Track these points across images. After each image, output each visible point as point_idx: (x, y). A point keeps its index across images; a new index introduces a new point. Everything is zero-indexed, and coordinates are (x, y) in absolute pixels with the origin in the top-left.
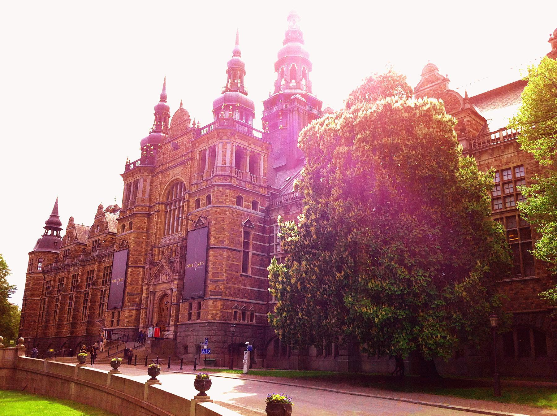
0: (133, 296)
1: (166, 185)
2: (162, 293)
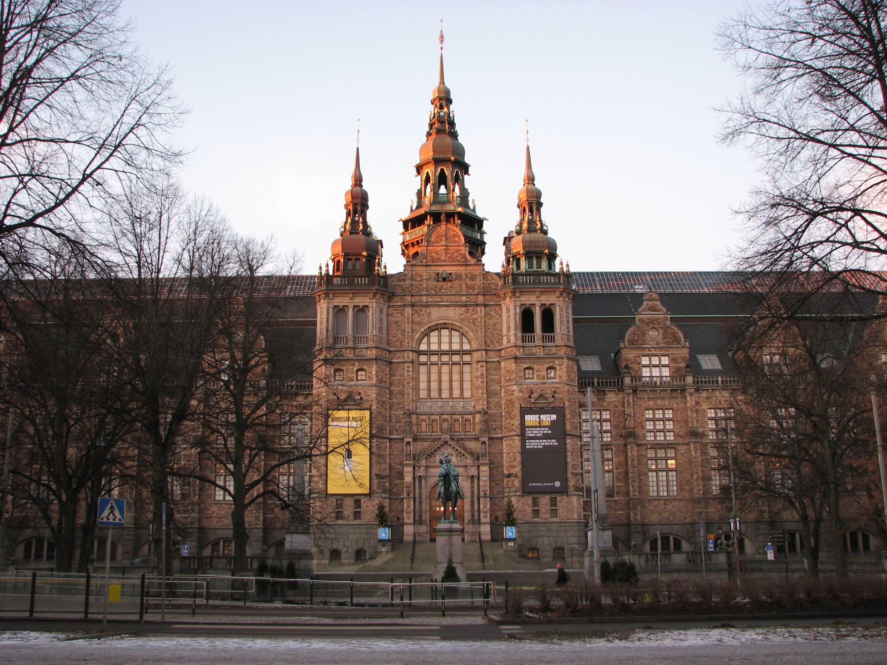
0: (382, 478)
1: (426, 327)
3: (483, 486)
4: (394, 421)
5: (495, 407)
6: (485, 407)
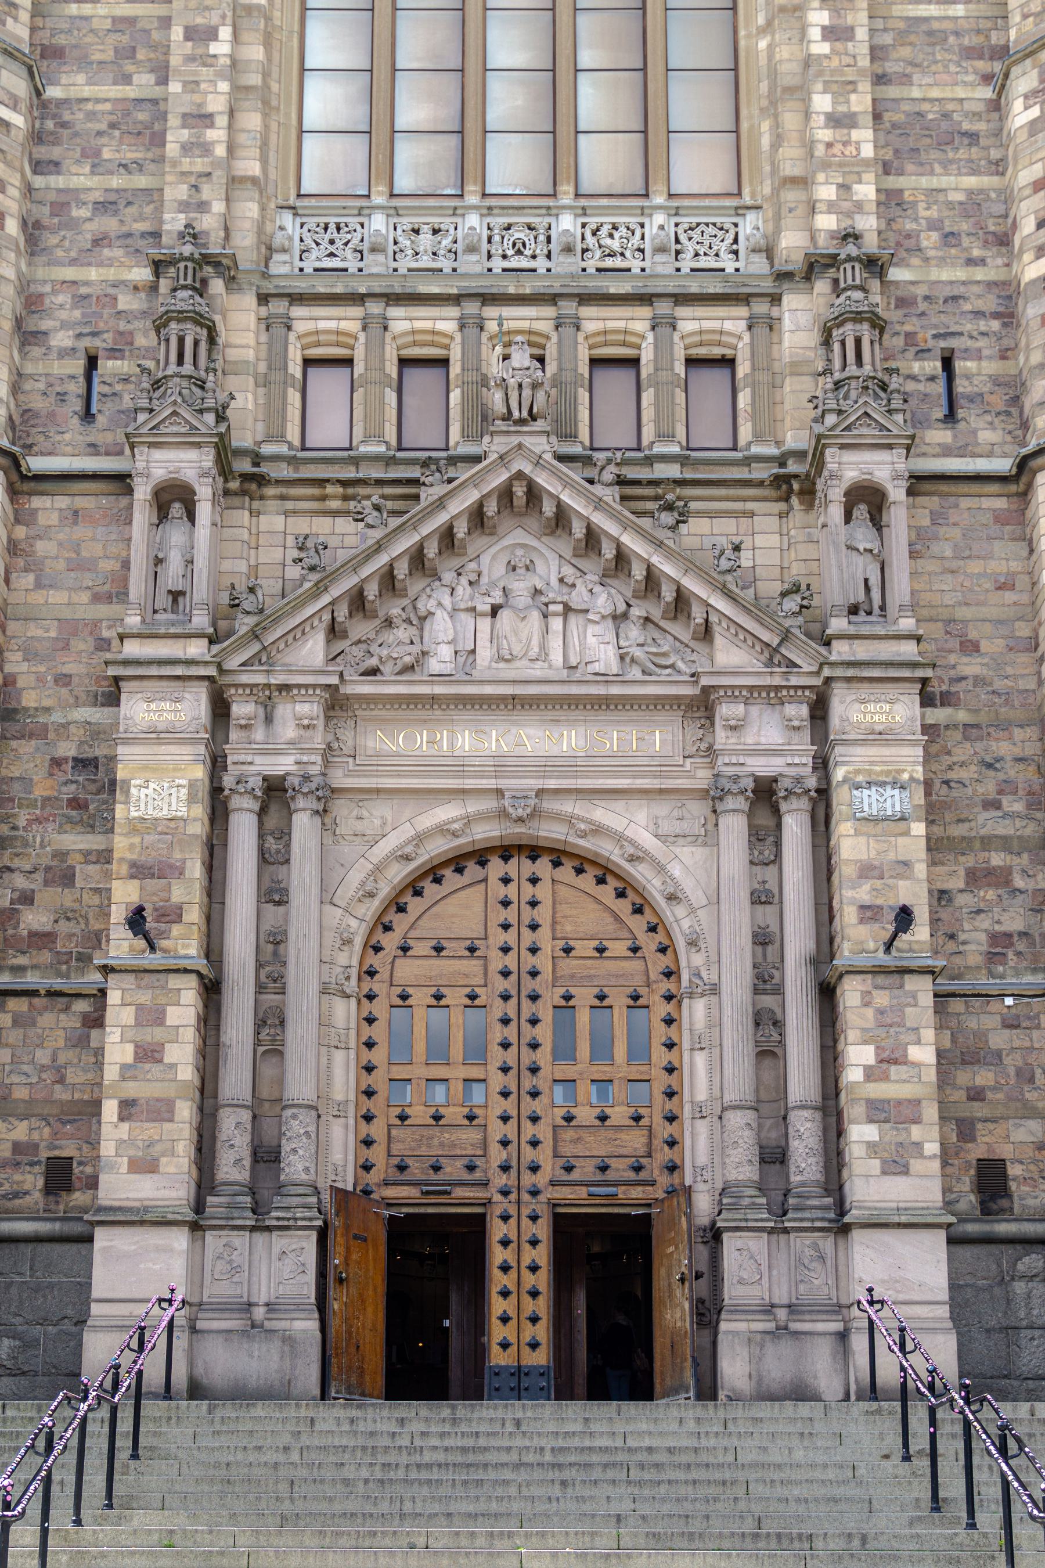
2: (469, 821)
3: (867, 871)
4: (62, 339)
5: (950, 238)
6: (868, 223)
